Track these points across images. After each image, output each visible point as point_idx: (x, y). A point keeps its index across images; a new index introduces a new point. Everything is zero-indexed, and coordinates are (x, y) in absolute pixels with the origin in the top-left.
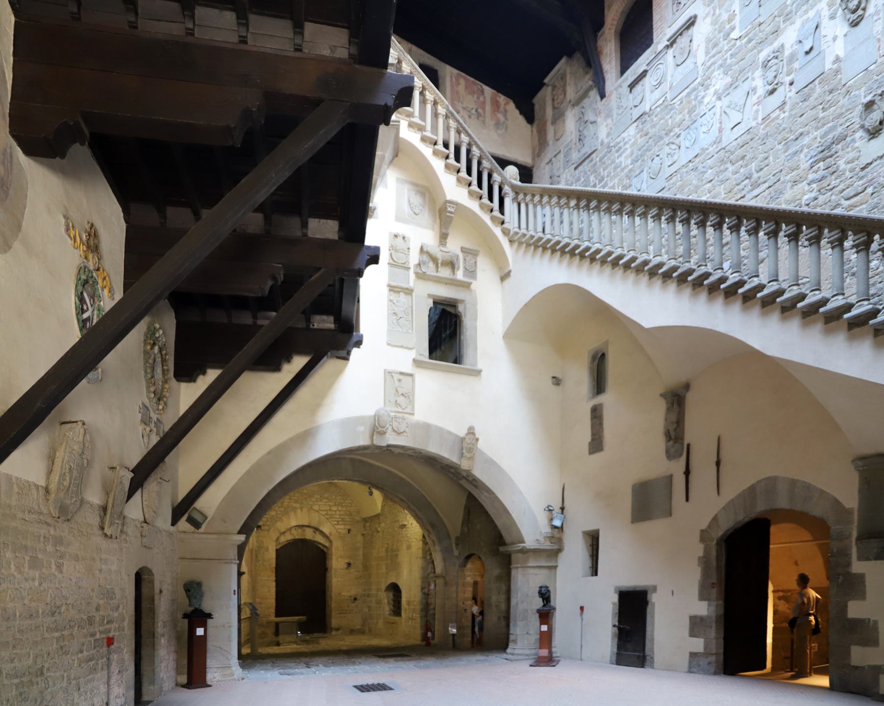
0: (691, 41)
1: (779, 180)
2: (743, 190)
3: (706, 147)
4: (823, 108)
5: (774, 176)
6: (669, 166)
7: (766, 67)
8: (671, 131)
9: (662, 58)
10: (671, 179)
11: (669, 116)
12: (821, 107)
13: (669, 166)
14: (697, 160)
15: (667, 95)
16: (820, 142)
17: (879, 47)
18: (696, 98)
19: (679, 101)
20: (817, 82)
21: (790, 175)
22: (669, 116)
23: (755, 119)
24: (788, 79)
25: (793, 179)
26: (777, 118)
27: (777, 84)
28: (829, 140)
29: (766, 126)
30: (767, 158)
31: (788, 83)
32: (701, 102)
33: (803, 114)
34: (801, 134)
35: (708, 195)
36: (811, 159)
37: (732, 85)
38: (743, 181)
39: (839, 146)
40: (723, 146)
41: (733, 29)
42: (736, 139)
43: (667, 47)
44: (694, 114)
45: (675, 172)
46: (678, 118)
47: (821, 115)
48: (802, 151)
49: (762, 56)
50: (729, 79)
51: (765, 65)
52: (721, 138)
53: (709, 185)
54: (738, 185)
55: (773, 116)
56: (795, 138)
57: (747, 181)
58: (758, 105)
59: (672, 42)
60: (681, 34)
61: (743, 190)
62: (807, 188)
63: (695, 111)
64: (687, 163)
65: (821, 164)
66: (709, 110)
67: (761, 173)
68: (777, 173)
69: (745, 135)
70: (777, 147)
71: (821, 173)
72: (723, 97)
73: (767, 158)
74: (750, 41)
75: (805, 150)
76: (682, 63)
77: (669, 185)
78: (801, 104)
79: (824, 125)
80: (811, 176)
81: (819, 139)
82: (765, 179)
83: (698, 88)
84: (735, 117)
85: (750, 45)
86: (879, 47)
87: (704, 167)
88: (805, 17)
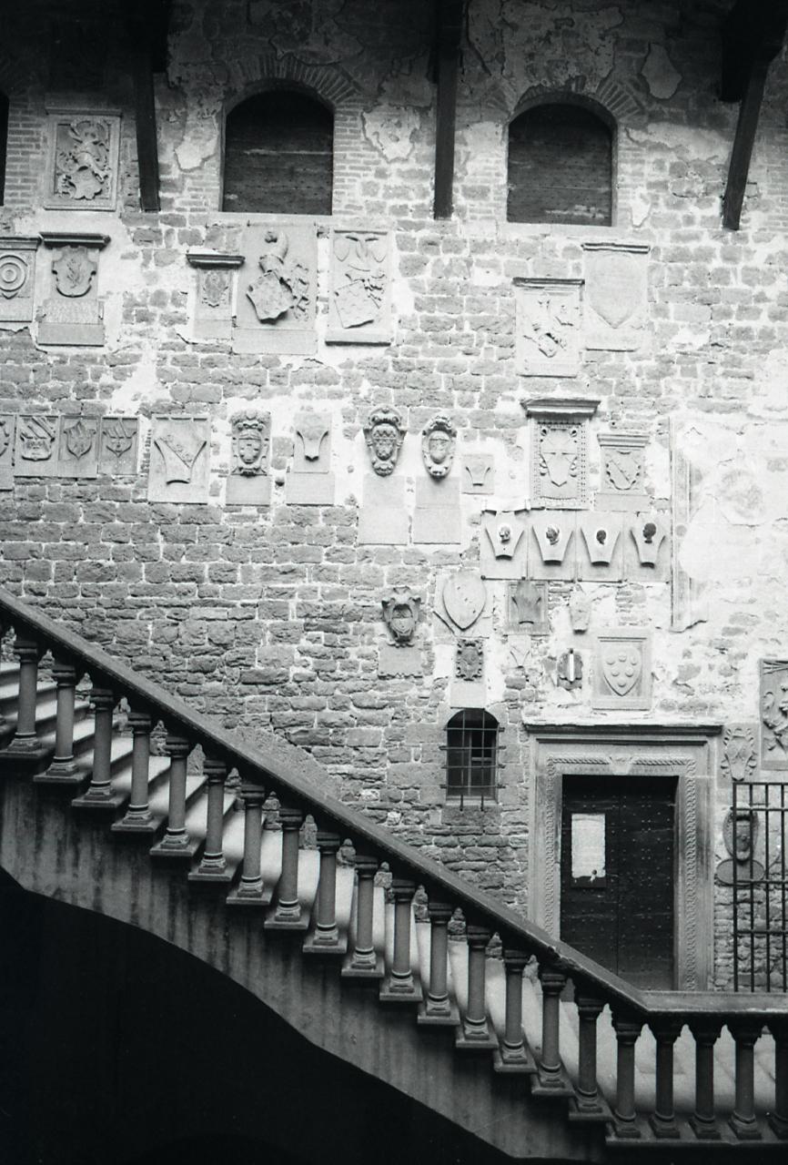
0: (94, 273)
1: (251, 618)
2: (185, 594)
3: (114, 477)
4: (327, 554)
5: (243, 605)
6: (24, 458)
7: (240, 429)
8: (34, 395)
9: (27, 253)
10: (28, 483)
11: (31, 366)
12: (325, 550)
13: (24, 458)
14: (91, 487)
15: (29, 325)
16: (321, 601)
17: (410, 528)
18: (97, 377)
19: (58, 355)
20: (321, 510)
21: (271, 622)
22: (31, 366)
23: (215, 494)
24: (276, 474)
25: (278, 630)
26: (252, 519)
27: (257, 470)
28: (335, 608)
29: (233, 519)
30: (231, 570)
31: (274, 479)
32: (107, 391)
33: (297, 543)
34: (292, 571)
35: (112, 563)
36: (307, 616)
37: (170, 409)
38: (184, 580)
39: (351, 625)
40: (150, 499)
41: (182, 320)
42: (177, 504)
43: (38, 241)
44: (89, 401)
45: (39, 477)
46: (53, 384)
47: (325, 563)
48: (291, 596)
49: (236, 405)
50: (166, 395)
51: (239, 425)
52: (146, 482)
53: (113, 545)
54: (174, 580)
55: (245, 511)
56: (281, 570)
57: (192, 584)
58: (220, 476)
59: (52, 242)
60: (74, 245)
61: (185, 594)
62: (297, 656)
63: (91, 398)
64: (68, 479)
65: (322, 634)
66: (124, 419)
67: (220, 587)
68: (249, 605)
69: (192, 507)
70: (250, 563)
71: (318, 648)
72: (154, 416)
73: (231, 570)
74: (211, 363)
75: (297, 600)
76: (70, 296)
77: (21, 491)
78: (293, 525)
79: (328, 580)
80: (304, 643)
81: (320, 597)
82: (227, 601)
83: (101, 363)
84: (176, 468)
85: (211, 371)
86: (410, 528)
87: (105, 508)
88: (307, 403)
